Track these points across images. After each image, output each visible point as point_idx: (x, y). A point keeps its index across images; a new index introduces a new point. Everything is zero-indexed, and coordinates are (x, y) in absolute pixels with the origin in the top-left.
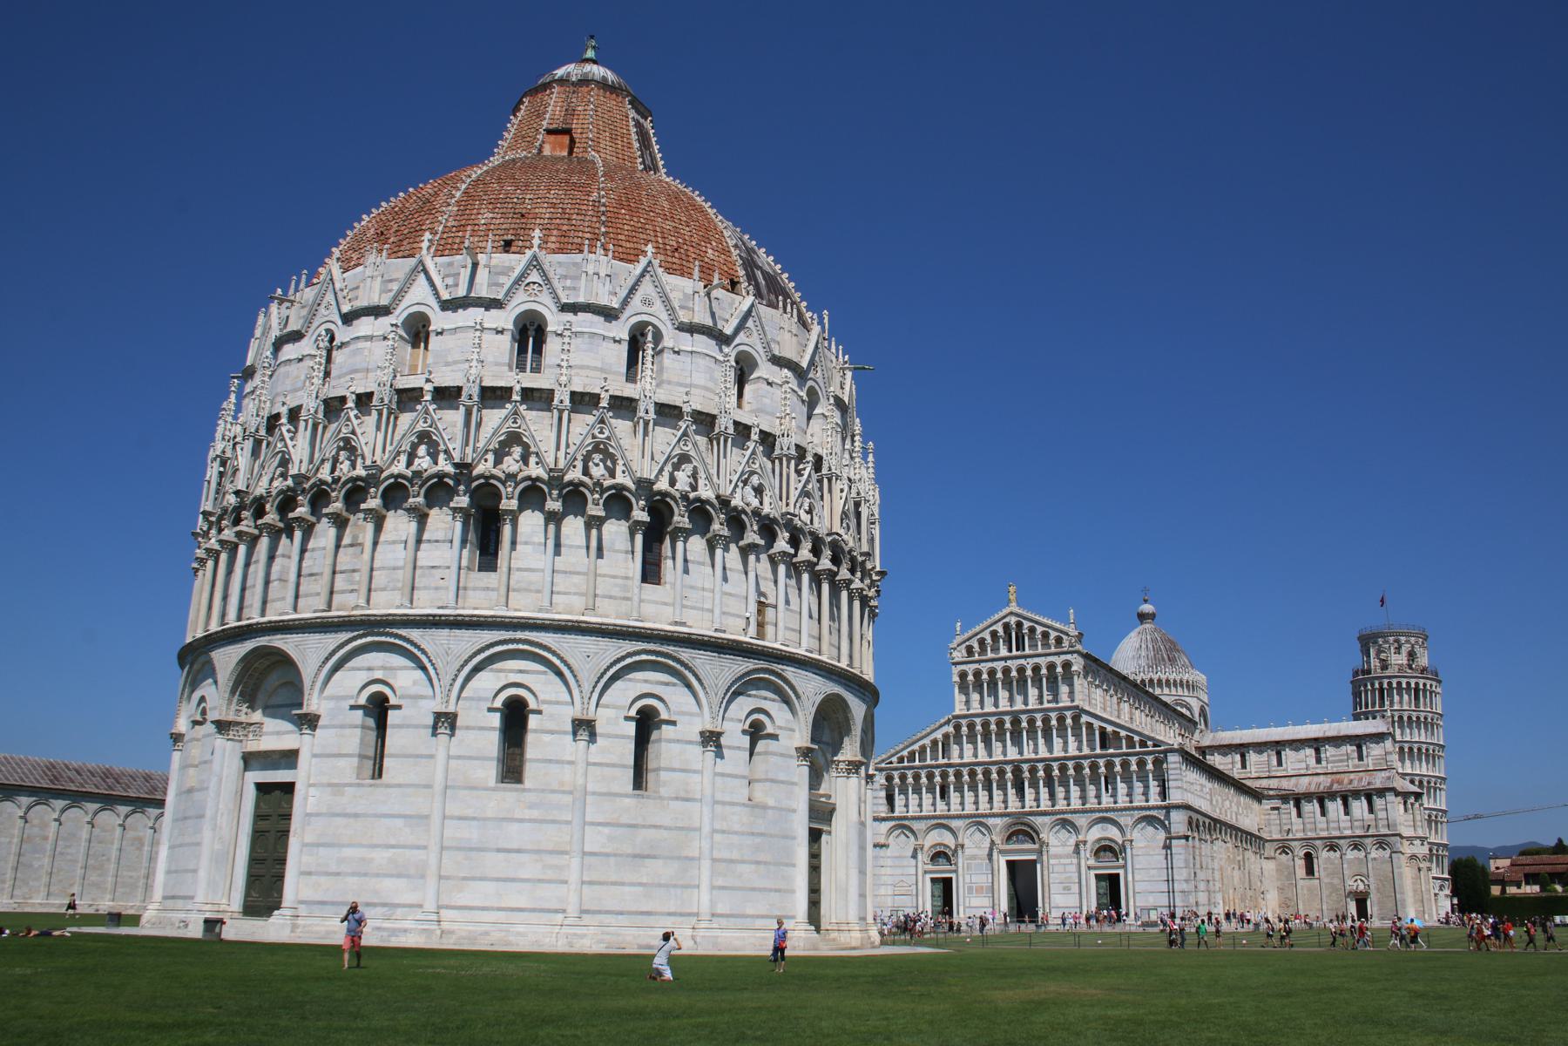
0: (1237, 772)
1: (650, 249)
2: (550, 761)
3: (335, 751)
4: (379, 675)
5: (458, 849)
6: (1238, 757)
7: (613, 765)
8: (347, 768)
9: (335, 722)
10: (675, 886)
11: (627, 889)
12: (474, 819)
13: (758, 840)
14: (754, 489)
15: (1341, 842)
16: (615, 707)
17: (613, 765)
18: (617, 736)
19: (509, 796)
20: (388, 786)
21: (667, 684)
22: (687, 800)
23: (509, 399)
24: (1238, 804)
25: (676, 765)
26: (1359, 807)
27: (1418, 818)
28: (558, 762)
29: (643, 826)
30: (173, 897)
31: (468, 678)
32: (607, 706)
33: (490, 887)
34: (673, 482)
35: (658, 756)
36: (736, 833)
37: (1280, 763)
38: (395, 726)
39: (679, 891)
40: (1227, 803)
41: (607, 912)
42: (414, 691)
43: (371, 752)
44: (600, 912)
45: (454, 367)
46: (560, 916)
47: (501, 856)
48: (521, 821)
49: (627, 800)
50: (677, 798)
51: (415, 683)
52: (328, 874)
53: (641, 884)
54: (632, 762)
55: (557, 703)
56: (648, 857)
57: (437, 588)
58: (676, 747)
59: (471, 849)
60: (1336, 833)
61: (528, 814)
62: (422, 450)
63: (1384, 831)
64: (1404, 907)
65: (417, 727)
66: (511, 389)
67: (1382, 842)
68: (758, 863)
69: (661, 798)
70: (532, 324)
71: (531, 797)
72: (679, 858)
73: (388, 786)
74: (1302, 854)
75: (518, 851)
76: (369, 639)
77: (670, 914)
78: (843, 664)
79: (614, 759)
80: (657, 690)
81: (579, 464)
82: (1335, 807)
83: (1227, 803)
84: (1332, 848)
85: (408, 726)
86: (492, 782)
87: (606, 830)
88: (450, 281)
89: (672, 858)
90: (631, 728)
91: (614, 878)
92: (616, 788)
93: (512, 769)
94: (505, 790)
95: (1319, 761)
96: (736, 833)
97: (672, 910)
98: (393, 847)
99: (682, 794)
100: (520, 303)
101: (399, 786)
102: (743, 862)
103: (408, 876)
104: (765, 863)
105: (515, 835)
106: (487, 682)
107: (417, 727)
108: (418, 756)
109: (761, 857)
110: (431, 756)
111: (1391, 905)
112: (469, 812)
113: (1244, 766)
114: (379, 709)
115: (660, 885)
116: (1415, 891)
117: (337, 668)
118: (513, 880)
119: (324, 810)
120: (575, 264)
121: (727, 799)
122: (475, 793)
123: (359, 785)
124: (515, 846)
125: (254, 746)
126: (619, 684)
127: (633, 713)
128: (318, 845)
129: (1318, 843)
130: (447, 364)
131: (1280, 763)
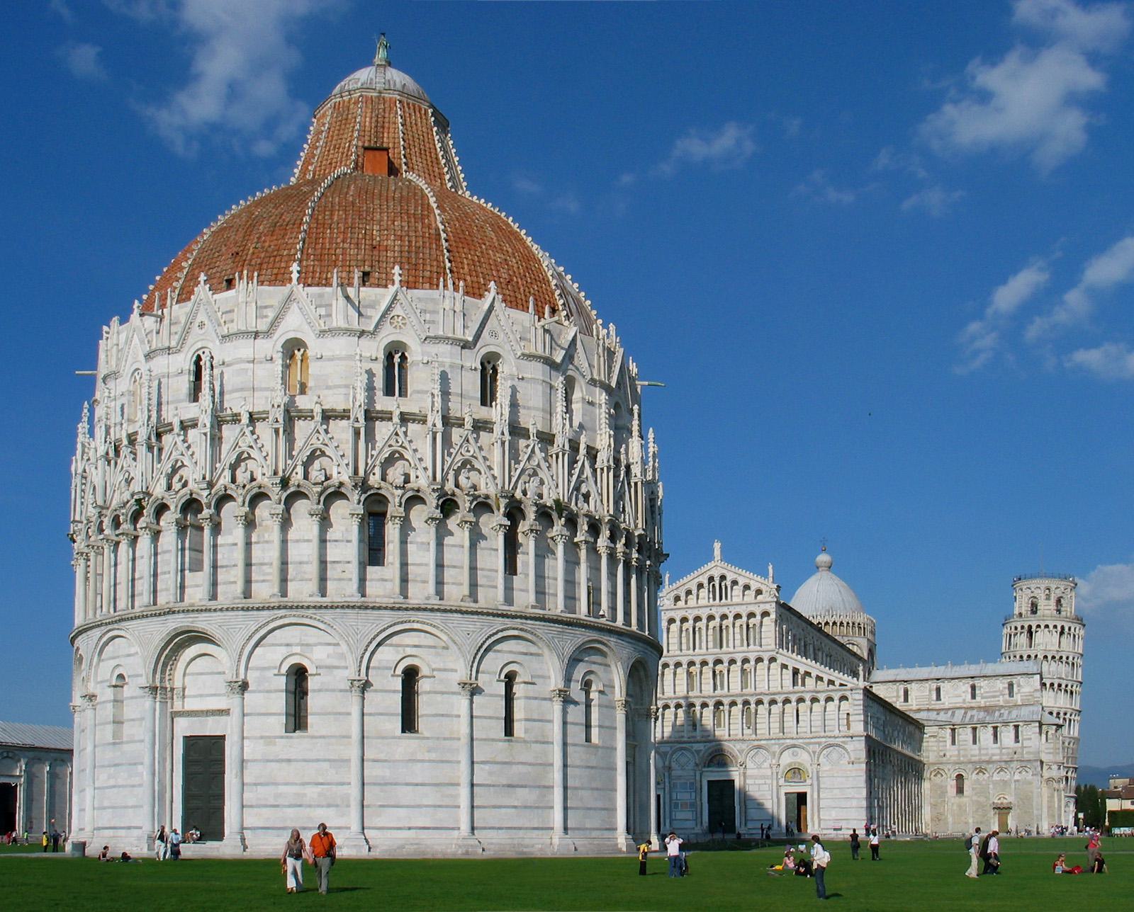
0: (899, 704)
2: (443, 715)
3: (263, 711)
4: (297, 649)
5: (375, 784)
6: (902, 693)
7: (490, 718)
8: (278, 723)
9: (261, 688)
10: (537, 808)
11: (503, 810)
12: (386, 761)
13: (593, 771)
17: (490, 718)
19: (409, 743)
20: (313, 737)
22: (544, 743)
23: (390, 419)
26: (1007, 735)
28: (447, 716)
29: (514, 763)
30: (99, 829)
31: (373, 653)
32: (483, 672)
33: (402, 812)
36: (577, 767)
37: (938, 698)
38: (314, 691)
39: (540, 811)
40: (896, 733)
42: (329, 662)
43: (293, 712)
45: (335, 391)
46: (456, 832)
47: (410, 788)
48: (423, 761)
49: (501, 743)
50: (536, 742)
51: (328, 656)
52: (266, 806)
53: (515, 807)
55: (445, 670)
57: (340, 580)
59: (386, 784)
60: (986, 758)
61: (427, 756)
63: (1026, 757)
65: (333, 690)
66: (391, 413)
67: (1024, 764)
71: (430, 743)
72: (539, 787)
73: (313, 737)
75: (422, 785)
76: (286, 621)
78: (634, 627)
79: (490, 713)
81: (451, 477)
82: (986, 735)
83: (896, 733)
84: (981, 771)
85: (327, 690)
87: (487, 767)
89: (535, 787)
92: (492, 736)
93: (409, 722)
94: (409, 738)
95: (974, 696)
96: (577, 767)
97: (536, 826)
98: (322, 784)
99: (540, 739)
100: (388, 335)
101: (323, 737)
102: (582, 789)
103: (337, 806)
104: (597, 789)
105: (420, 773)
106: (387, 655)
107: (333, 690)
108: (340, 714)
109: (594, 785)
110: (349, 714)
112: (382, 756)
113: (906, 700)
114: (299, 675)
115: (526, 807)
116: (1049, 807)
117: (257, 645)
118: (419, 806)
119: (259, 757)
120: (433, 300)
122: (386, 741)
123: (287, 737)
124: (419, 780)
125: (178, 706)
126: (491, 654)
128: (256, 784)
129: (970, 766)
130: (328, 388)
131: (938, 698)
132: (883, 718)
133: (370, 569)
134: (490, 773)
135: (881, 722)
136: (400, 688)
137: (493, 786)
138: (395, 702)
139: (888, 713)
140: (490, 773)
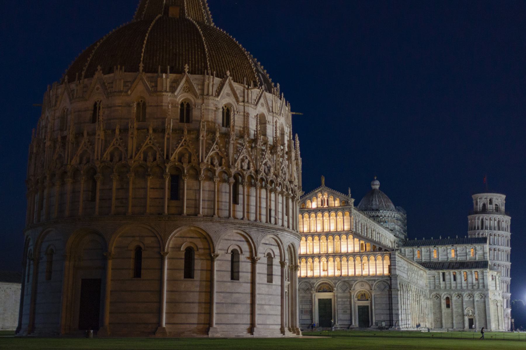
1: (228, 73)
11: (230, 315)
13: (270, 297)
14: (268, 167)
15: (463, 293)
16: (224, 250)
18: (225, 260)
21: (241, 241)
24: (418, 275)
25: (244, 270)
27: (498, 283)
29: (235, 293)
34: (242, 167)
35: (238, 267)
41: (223, 324)
44: (221, 324)
47: (187, 305)
49: (229, 283)
50: (245, 282)
54: (229, 269)
56: (236, 304)
58: (243, 263)
62: (150, 154)
64: (490, 323)
68: (270, 305)
69: (240, 283)
70: (185, 102)
74: (445, 297)
75: (193, 303)
77: (243, 324)
79: (224, 268)
80: (239, 243)
83: (413, 275)
86: (183, 278)
87: (222, 294)
88: (153, 84)
90: (229, 257)
91: (225, 312)
92: (225, 279)
96: (263, 294)
98: (147, 302)
104: (272, 305)
111: (483, 321)
116: (495, 316)
118: (191, 313)
121: (261, 282)
124: (191, 301)
127: (229, 251)
132: (407, 267)
133: (173, 201)
134: (224, 297)
135: (406, 269)
136: (183, 257)
137: (225, 303)
138: (181, 264)
139: (409, 264)
140: (224, 297)
